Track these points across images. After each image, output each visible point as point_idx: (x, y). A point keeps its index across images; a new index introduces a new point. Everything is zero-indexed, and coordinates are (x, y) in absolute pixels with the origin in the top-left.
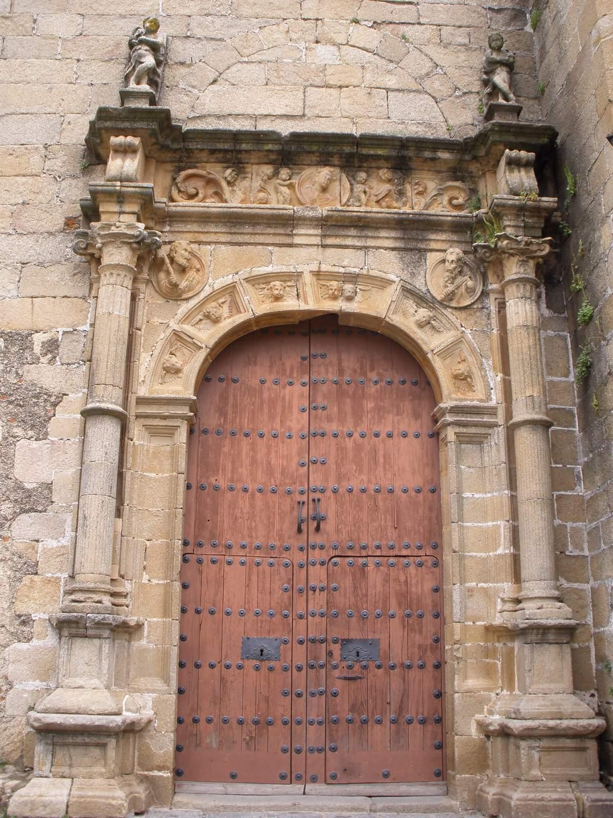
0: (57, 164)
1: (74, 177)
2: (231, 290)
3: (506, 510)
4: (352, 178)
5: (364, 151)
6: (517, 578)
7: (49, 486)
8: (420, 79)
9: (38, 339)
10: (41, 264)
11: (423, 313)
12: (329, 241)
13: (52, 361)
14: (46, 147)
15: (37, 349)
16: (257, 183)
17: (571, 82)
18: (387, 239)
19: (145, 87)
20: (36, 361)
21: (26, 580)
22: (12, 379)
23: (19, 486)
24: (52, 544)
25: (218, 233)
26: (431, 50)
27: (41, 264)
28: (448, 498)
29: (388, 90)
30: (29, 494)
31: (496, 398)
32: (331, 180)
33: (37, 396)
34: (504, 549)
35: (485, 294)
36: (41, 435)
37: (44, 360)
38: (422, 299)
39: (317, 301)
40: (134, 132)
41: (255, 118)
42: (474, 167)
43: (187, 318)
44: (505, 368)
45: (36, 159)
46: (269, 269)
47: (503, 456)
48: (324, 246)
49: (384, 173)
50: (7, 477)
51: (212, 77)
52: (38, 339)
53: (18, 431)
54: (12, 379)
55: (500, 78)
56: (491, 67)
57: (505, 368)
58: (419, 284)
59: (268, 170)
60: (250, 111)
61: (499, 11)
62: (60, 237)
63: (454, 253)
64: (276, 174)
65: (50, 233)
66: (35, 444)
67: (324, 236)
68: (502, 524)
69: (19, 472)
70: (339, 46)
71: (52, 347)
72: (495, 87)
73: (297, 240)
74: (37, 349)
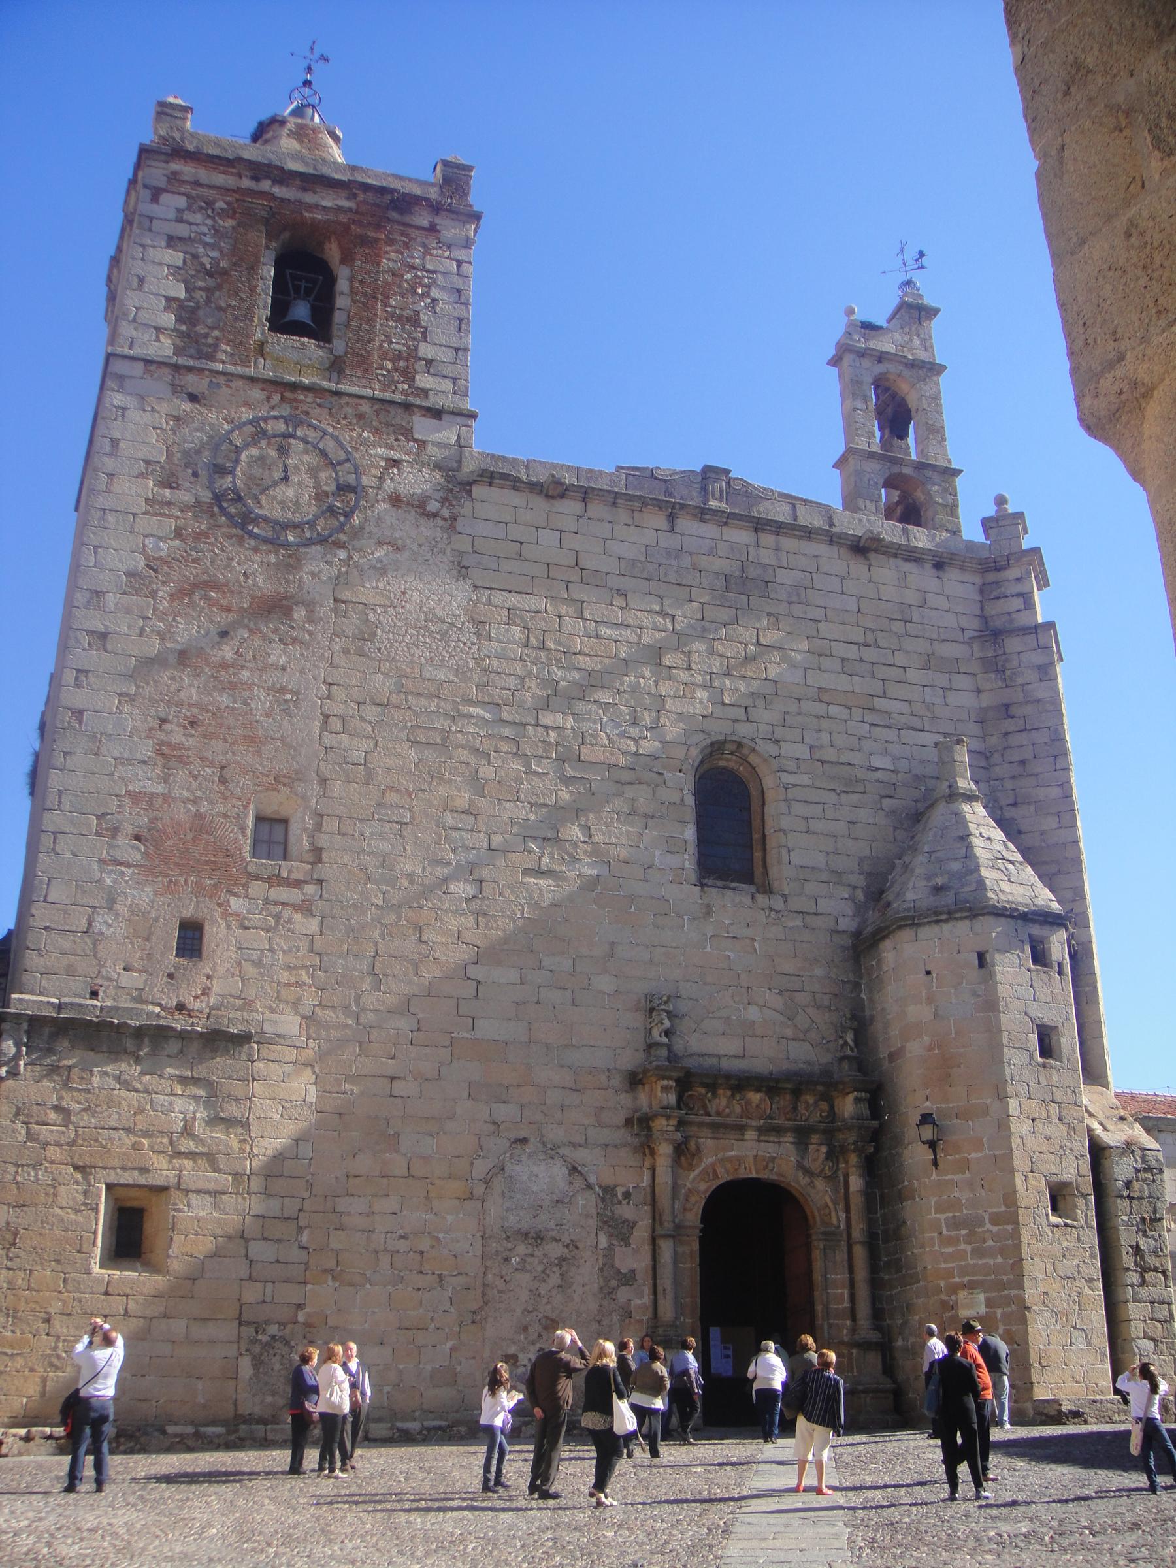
0: (617, 1081)
1: (627, 1092)
2: (713, 1165)
3: (847, 1283)
4: (771, 1099)
5: (781, 1085)
6: (854, 1318)
7: (633, 1271)
8: (805, 1032)
9: (620, 1191)
10: (616, 1146)
11: (807, 1179)
12: (762, 1138)
13: (628, 1203)
14: (609, 1070)
15: (620, 1196)
16: (724, 1102)
17: (892, 1057)
18: (789, 1138)
19: (665, 1040)
20: (620, 1203)
21: (627, 1321)
22: (609, 1213)
23: (619, 1272)
24: (639, 1302)
25: (707, 1132)
26: (811, 1011)
27: (616, 1146)
28: (817, 1277)
29: (787, 1039)
30: (625, 1275)
31: (843, 1226)
32: (761, 1100)
33: (623, 1223)
34: (847, 1304)
35: (837, 1170)
36: (628, 1245)
37: (624, 1202)
38: (808, 1172)
39: (757, 1172)
40: (669, 1078)
41: (719, 1057)
42: (834, 1094)
43: (694, 1179)
44: (847, 1210)
45: (603, 1078)
46: (733, 1153)
47: (846, 1257)
48: (759, 1141)
49: (788, 1097)
50: (613, 1266)
51: (694, 1026)
52: (620, 1191)
53: (615, 1242)
54: (609, 1213)
55: (849, 1038)
56: (844, 1029)
57: (847, 1210)
58: (805, 1163)
59: (729, 1093)
60: (716, 1052)
61: (848, 982)
62: (623, 1130)
63: (824, 1149)
64: (733, 1095)
65: (618, 1127)
66: (624, 1249)
67: (760, 1135)
68: (846, 1291)
69: (617, 1264)
70: (761, 1007)
71: (627, 1195)
72: (846, 1043)
73: (746, 1137)
74: (620, 1196)
